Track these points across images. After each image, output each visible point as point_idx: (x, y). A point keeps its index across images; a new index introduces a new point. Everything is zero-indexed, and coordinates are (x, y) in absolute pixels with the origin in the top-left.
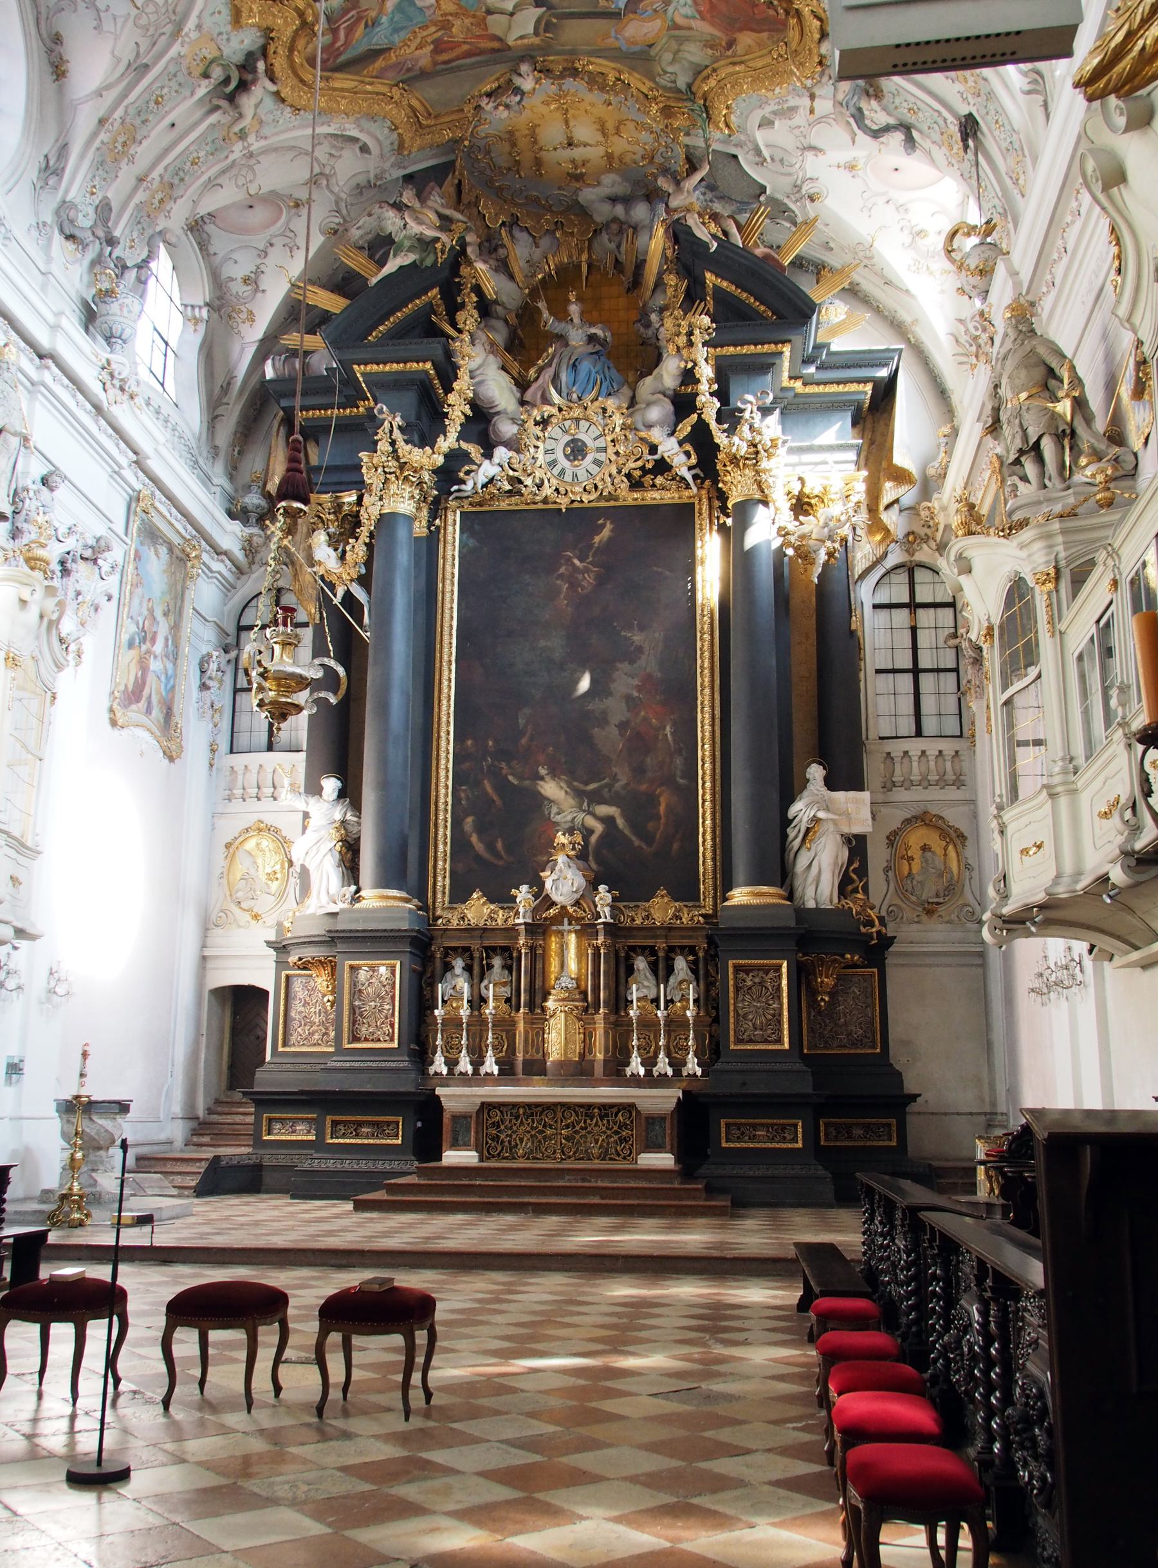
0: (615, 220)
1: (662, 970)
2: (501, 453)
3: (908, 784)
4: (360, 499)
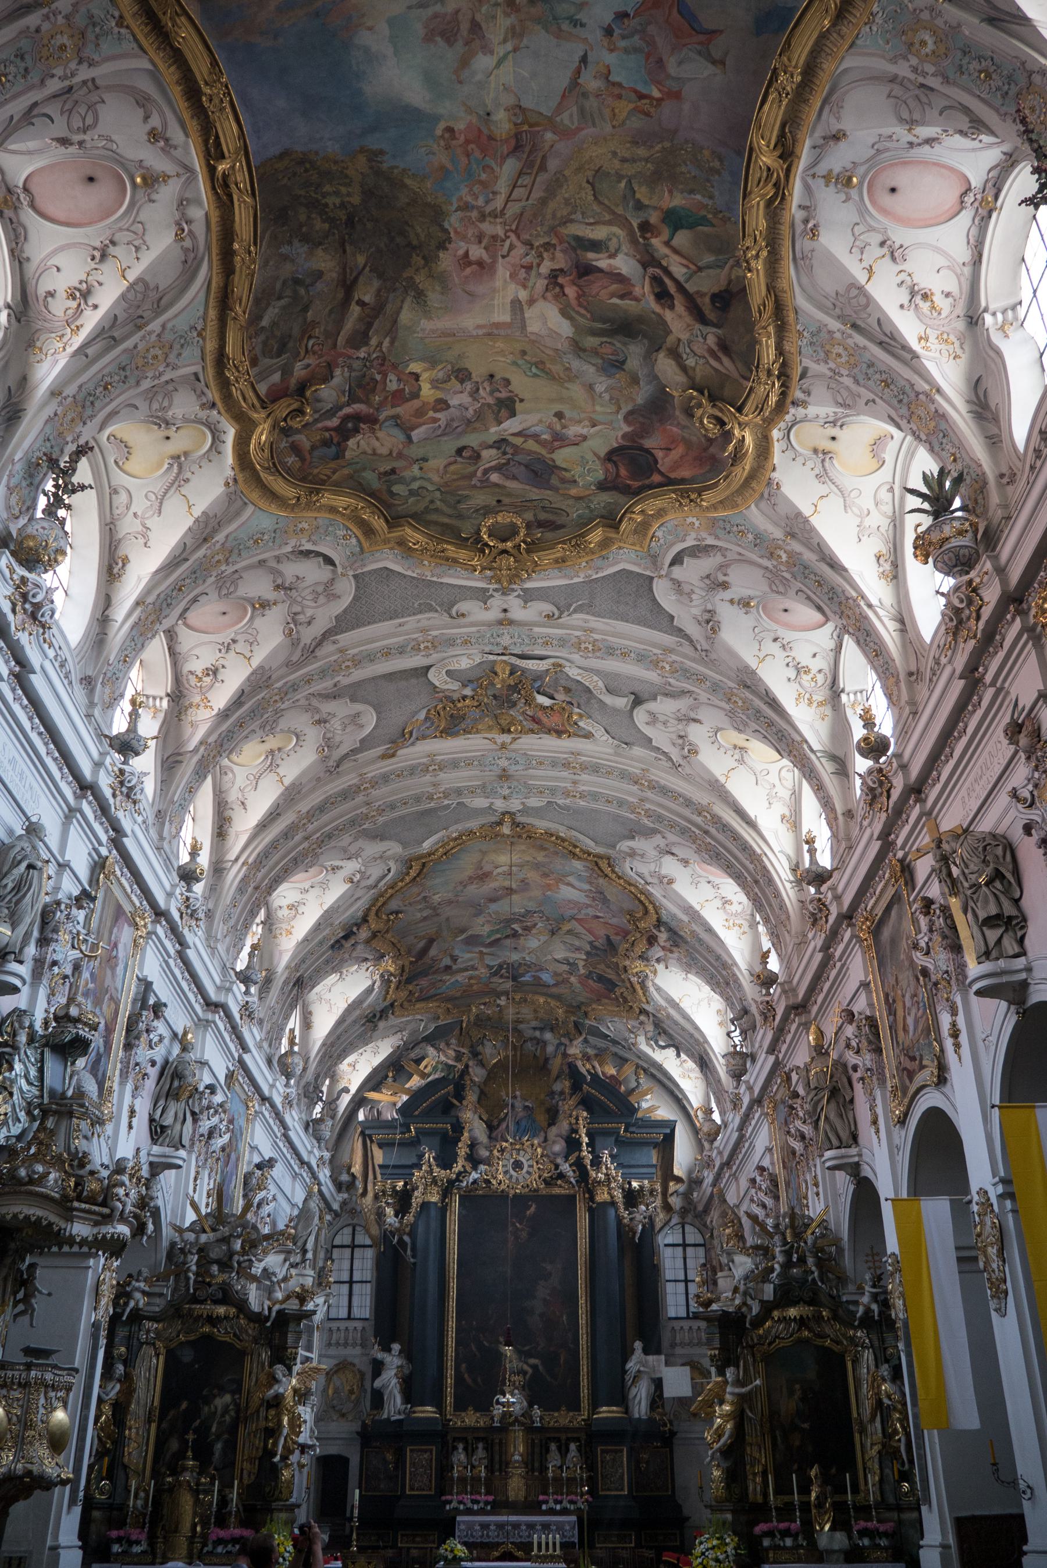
0: (535, 1038)
1: (564, 1451)
2: (482, 1167)
3: (683, 1345)
4: (406, 1184)
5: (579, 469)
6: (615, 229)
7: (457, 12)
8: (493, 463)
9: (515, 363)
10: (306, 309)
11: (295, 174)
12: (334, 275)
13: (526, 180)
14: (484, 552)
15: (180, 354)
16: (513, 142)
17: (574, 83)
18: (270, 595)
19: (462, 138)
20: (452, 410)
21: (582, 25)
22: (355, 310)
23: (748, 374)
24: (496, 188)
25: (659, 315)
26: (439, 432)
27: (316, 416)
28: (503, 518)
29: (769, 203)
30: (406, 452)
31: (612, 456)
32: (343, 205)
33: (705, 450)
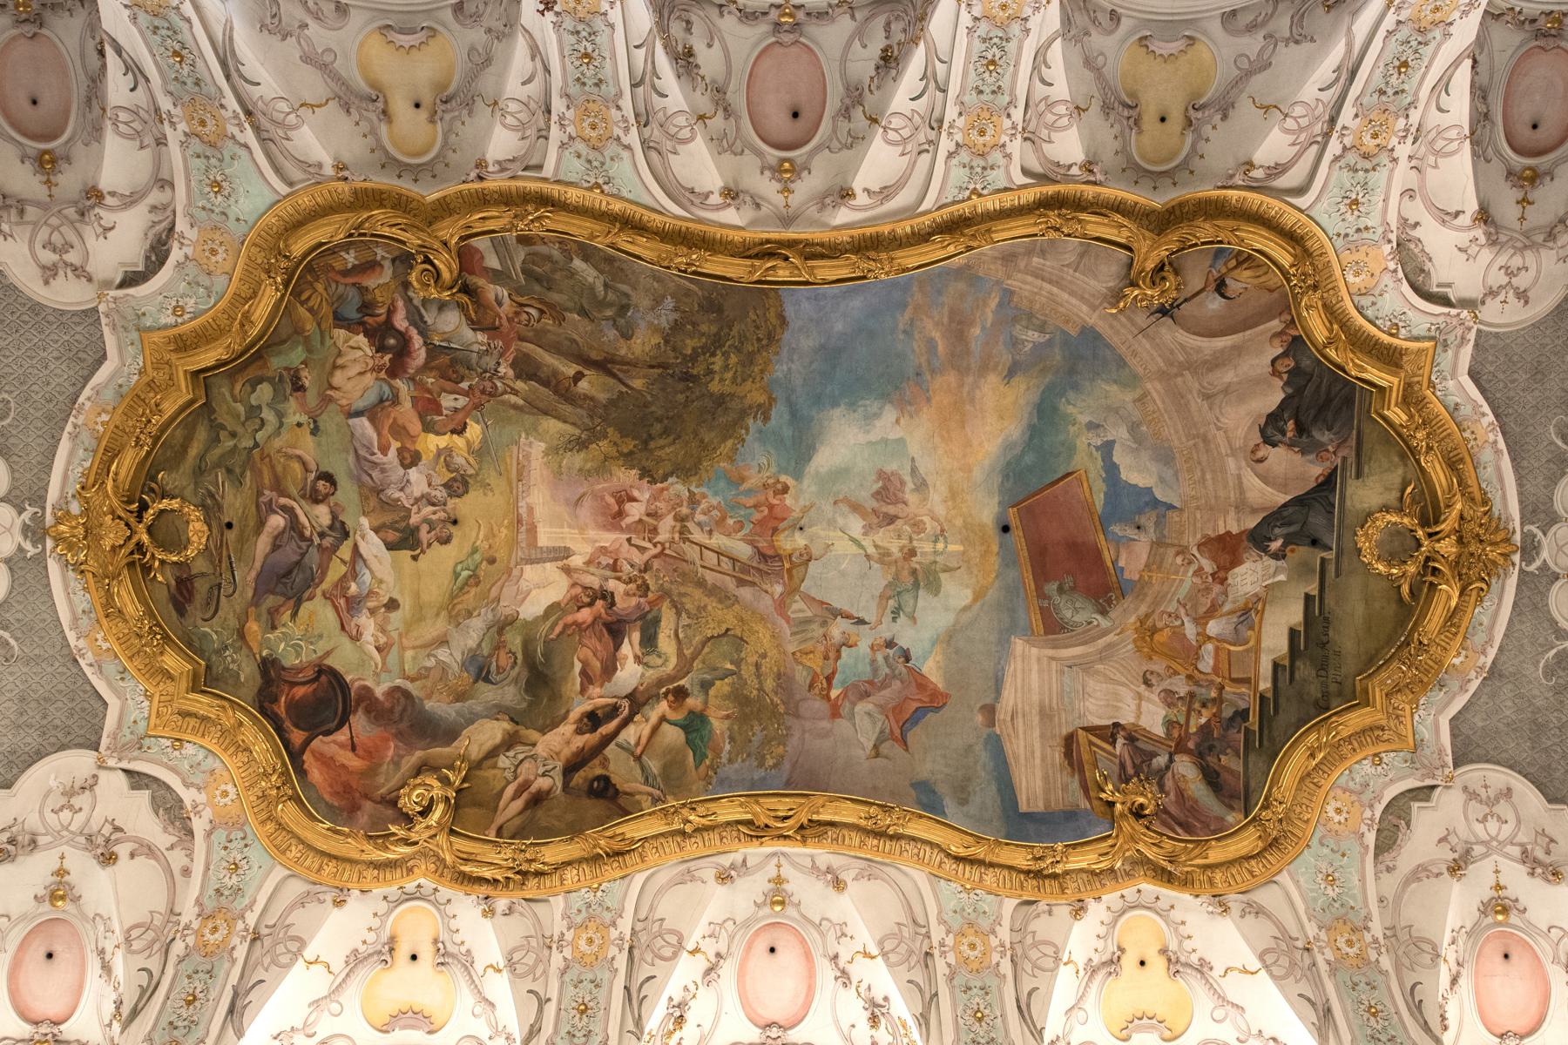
5: (298, 633)
6: (673, 661)
7: (905, 503)
8: (303, 519)
9: (475, 550)
10: (583, 312)
11: (757, 328)
12: (623, 352)
13: (726, 565)
14: (130, 502)
15: (579, 156)
16: (770, 552)
17: (837, 613)
18: (69, 181)
19: (775, 502)
20: (401, 471)
21: (894, 619)
22: (570, 369)
23: (505, 832)
24: (716, 535)
25: (565, 717)
26: (362, 452)
27: (416, 302)
28: (197, 531)
29: (749, 823)
30: (332, 407)
31: (328, 678)
32: (710, 372)
33: (366, 797)
